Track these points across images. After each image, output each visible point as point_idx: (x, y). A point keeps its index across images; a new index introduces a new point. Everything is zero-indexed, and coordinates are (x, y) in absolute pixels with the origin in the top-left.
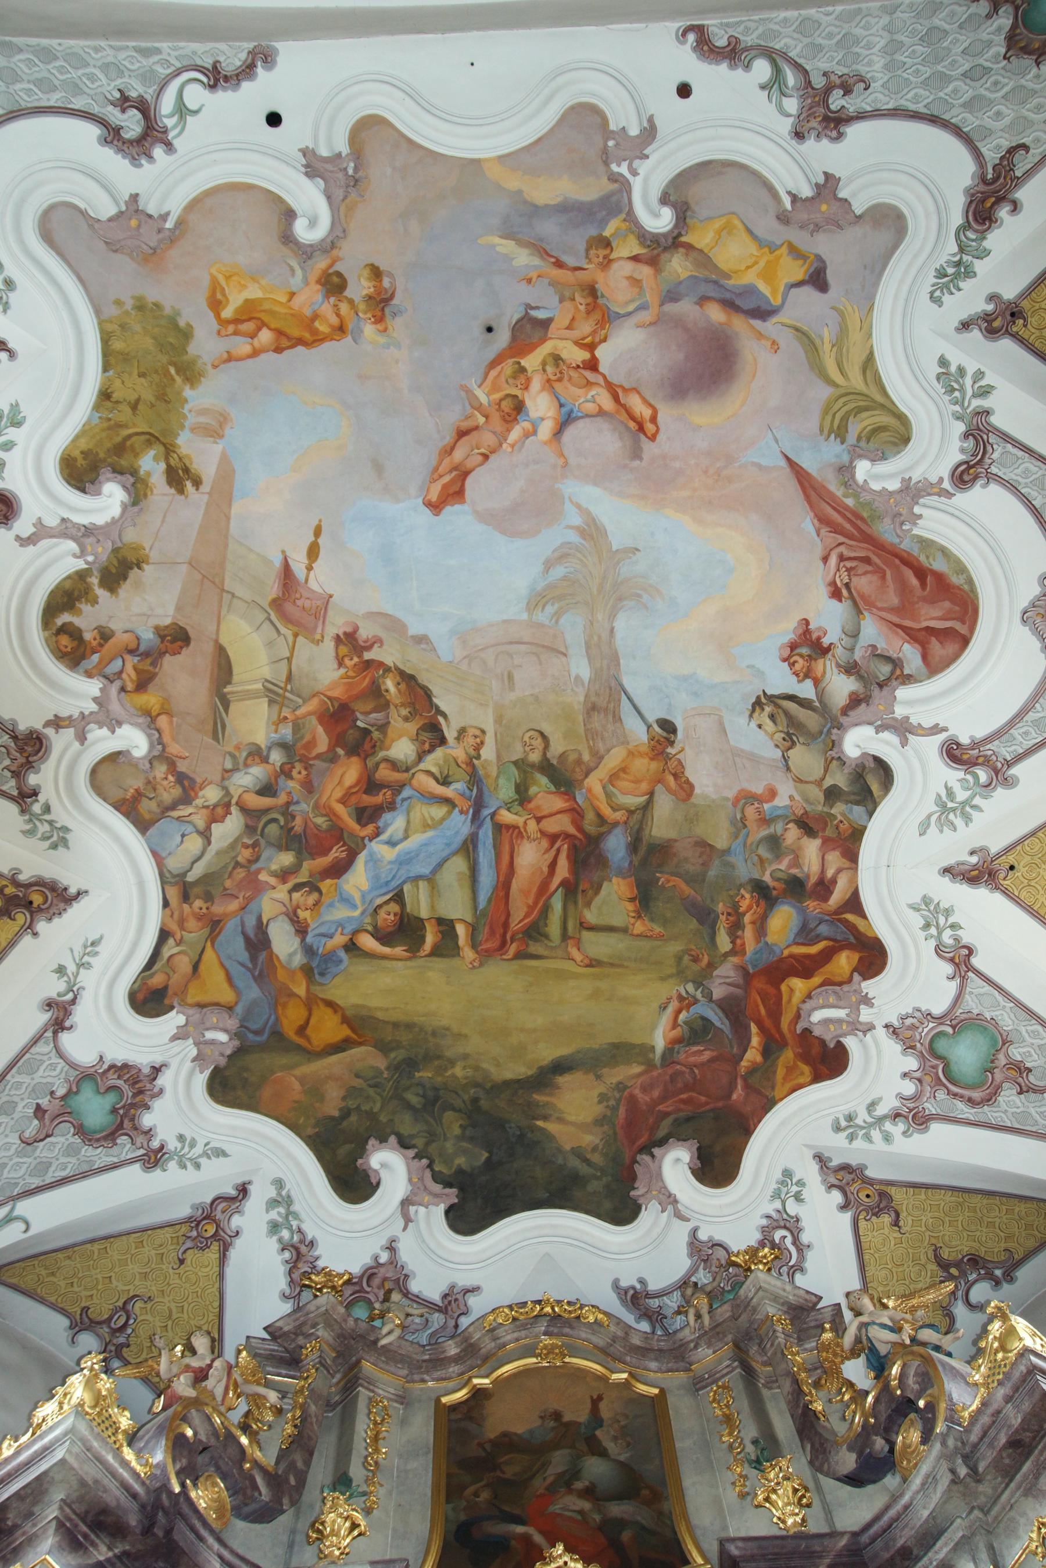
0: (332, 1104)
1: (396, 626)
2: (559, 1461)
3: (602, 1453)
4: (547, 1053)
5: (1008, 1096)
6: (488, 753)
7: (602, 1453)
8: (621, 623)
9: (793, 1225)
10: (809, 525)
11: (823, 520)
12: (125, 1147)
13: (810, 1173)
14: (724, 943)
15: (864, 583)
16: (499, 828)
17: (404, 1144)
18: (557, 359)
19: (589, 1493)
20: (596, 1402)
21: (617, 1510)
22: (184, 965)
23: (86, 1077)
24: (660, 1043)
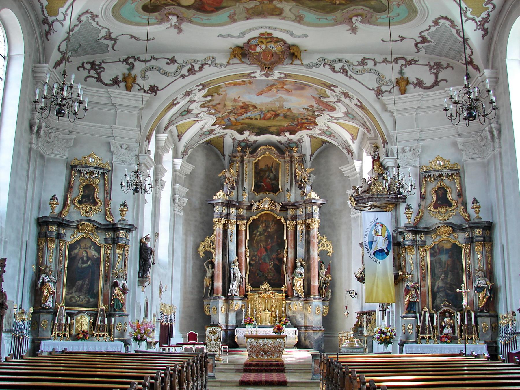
0: (239, 128)
1: (252, 102)
2: (267, 173)
3: (272, 172)
4: (270, 125)
5: (332, 137)
6: (264, 109)
7: (272, 172)
8: (284, 103)
9: (302, 140)
10: (313, 99)
11: (315, 100)
12: (211, 134)
13: (305, 136)
14: (296, 121)
15: (320, 104)
16: (264, 114)
17: (249, 130)
18: (277, 87)
19: (270, 179)
20: (273, 163)
21: (273, 182)
22: (219, 122)
23: (205, 132)
24: (286, 125)
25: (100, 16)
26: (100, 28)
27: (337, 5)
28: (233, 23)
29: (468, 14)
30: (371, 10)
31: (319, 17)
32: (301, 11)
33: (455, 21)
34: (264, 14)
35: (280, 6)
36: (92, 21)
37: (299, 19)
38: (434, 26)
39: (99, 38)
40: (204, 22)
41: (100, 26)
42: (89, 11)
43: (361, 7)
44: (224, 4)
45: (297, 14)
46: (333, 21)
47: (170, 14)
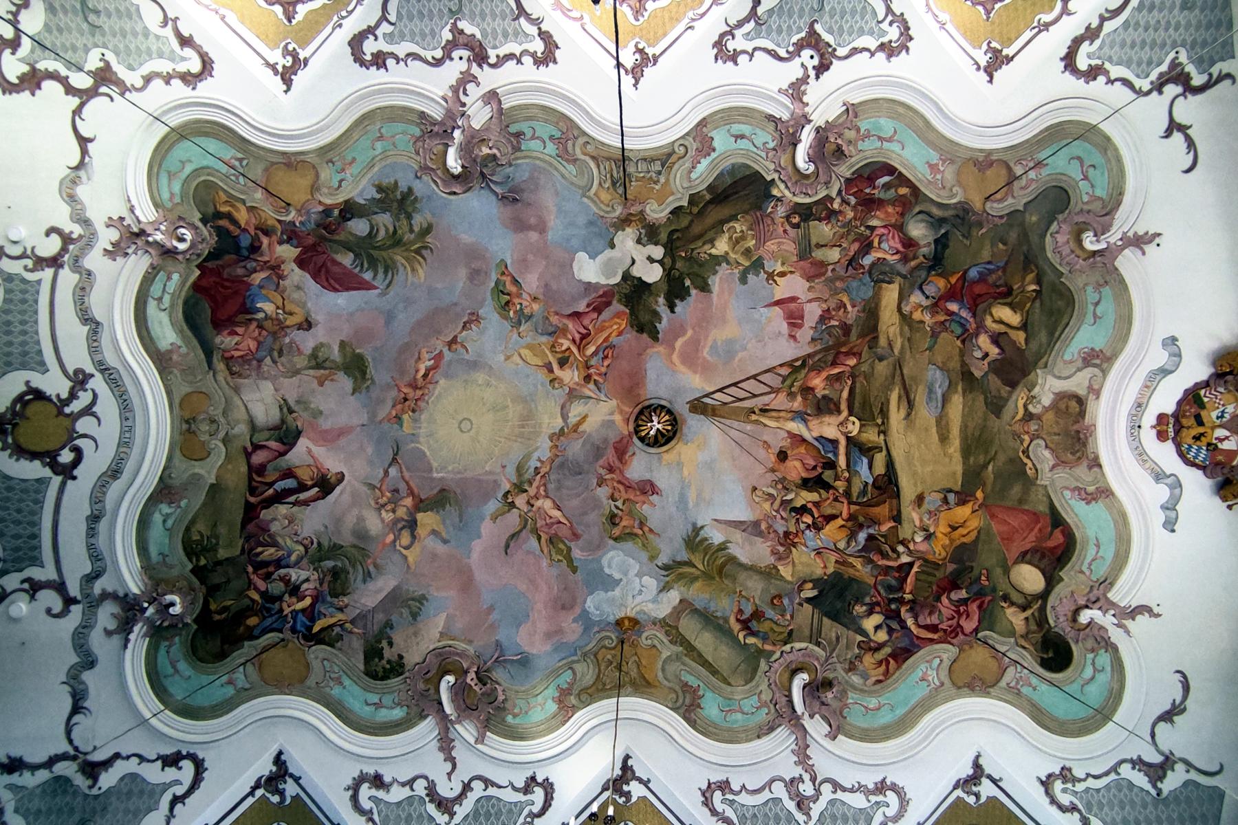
25: (1068, 764)
26: (1113, 776)
27: (1040, 287)
28: (1112, 494)
29: (1046, 18)
30: (1060, 217)
31: (1091, 320)
32: (1067, 357)
33: (1072, 37)
34: (1078, 432)
35: (1047, 400)
36: (1080, 787)
37: (1099, 360)
38: (1106, 73)
39: (1153, 792)
40: (1108, 552)
41: (1107, 774)
42: (1044, 779)
43: (1048, 238)
44: (1043, 508)
45: (1080, 363)
46: (1106, 291)
47: (1075, 620)
